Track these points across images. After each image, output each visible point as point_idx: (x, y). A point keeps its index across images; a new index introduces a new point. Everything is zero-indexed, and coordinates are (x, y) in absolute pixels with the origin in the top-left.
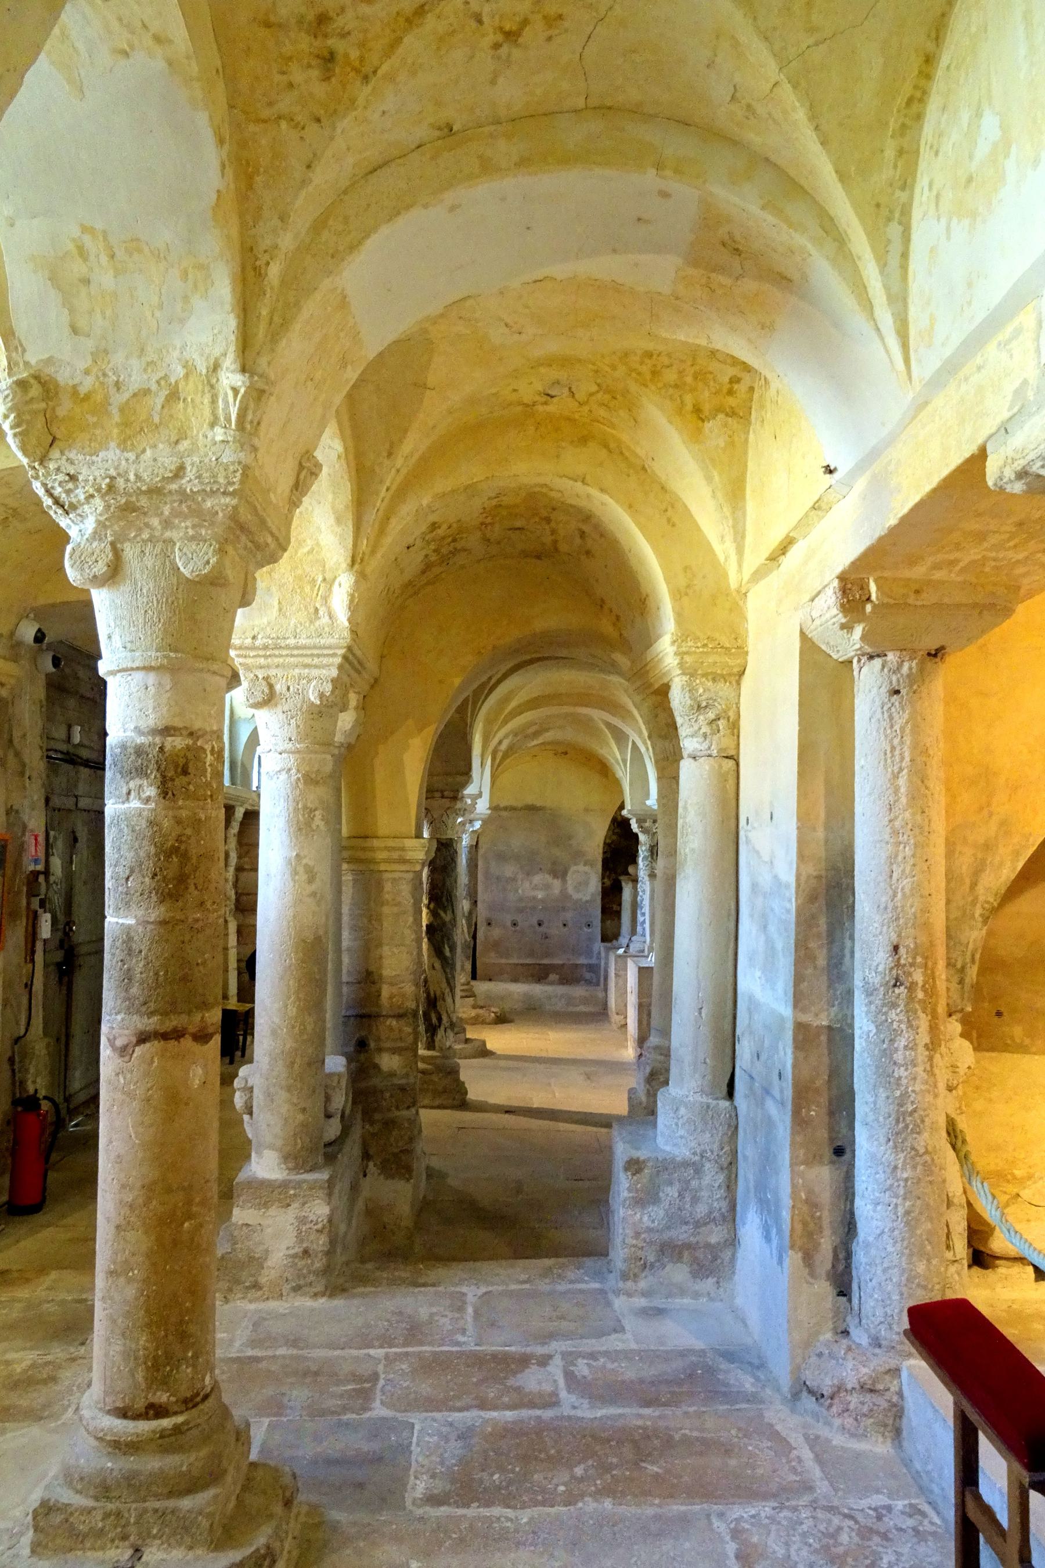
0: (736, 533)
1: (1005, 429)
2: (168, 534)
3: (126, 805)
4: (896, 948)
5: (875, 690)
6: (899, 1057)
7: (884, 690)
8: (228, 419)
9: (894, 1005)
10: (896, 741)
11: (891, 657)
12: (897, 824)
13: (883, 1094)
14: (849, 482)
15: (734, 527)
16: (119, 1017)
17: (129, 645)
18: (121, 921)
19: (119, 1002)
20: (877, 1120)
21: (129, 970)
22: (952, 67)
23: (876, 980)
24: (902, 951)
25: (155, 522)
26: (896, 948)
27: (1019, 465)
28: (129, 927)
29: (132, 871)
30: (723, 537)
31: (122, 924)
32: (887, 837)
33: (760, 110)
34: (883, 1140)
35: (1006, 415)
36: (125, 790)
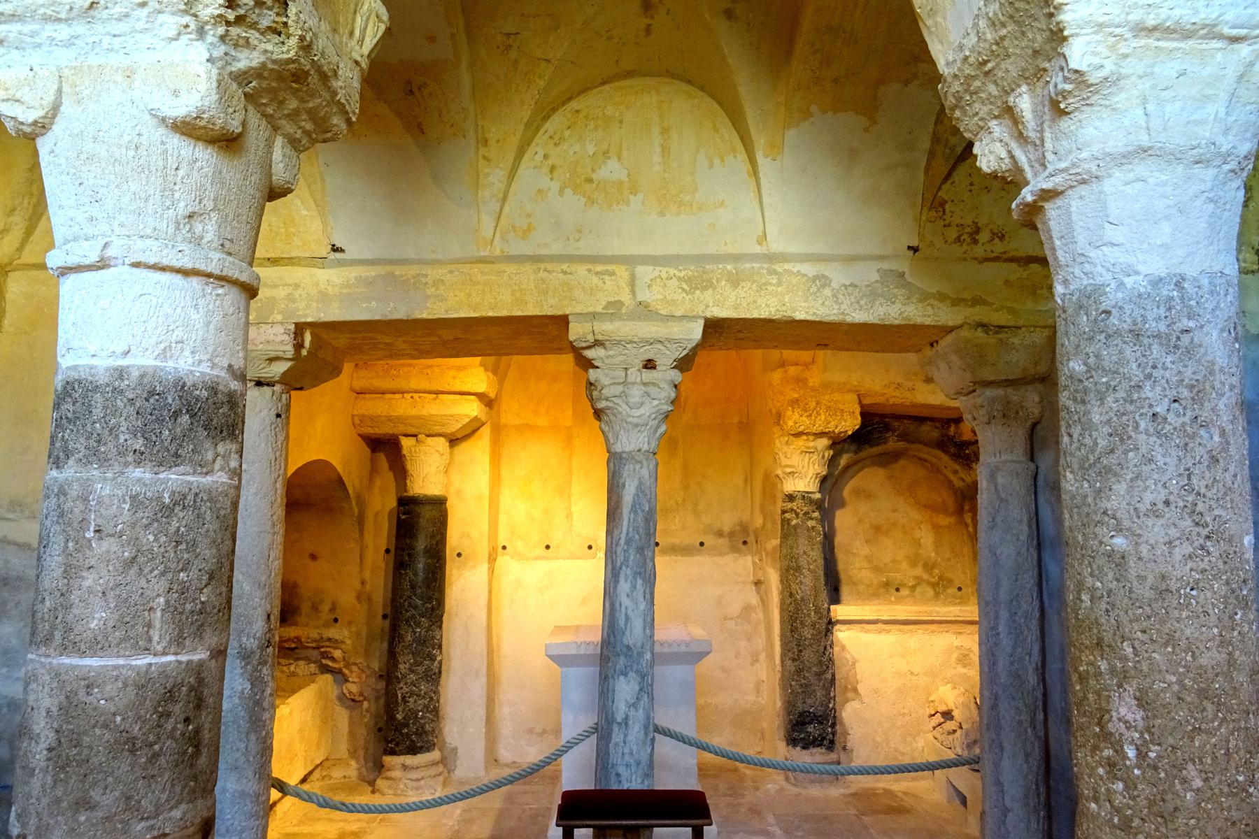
0: (34, 212)
1: (594, 316)
2: (283, 122)
3: (209, 478)
4: (269, 616)
5: (265, 412)
6: (265, 704)
7: (273, 412)
8: (361, 42)
9: (265, 663)
10: (278, 454)
11: (278, 388)
12: (275, 517)
13: (253, 737)
14: (341, 264)
15: (35, 206)
16: (177, 813)
17: (227, 244)
18: (183, 658)
19: (178, 789)
20: (248, 761)
21: (197, 731)
22: (581, 115)
23: (251, 644)
24: (272, 617)
25: (293, 104)
26: (269, 616)
27: (600, 337)
28: (201, 664)
29: (211, 578)
30: (14, 210)
31: (189, 662)
32: (268, 527)
33: (513, 54)
34: (250, 774)
35: (599, 309)
36: (210, 456)
